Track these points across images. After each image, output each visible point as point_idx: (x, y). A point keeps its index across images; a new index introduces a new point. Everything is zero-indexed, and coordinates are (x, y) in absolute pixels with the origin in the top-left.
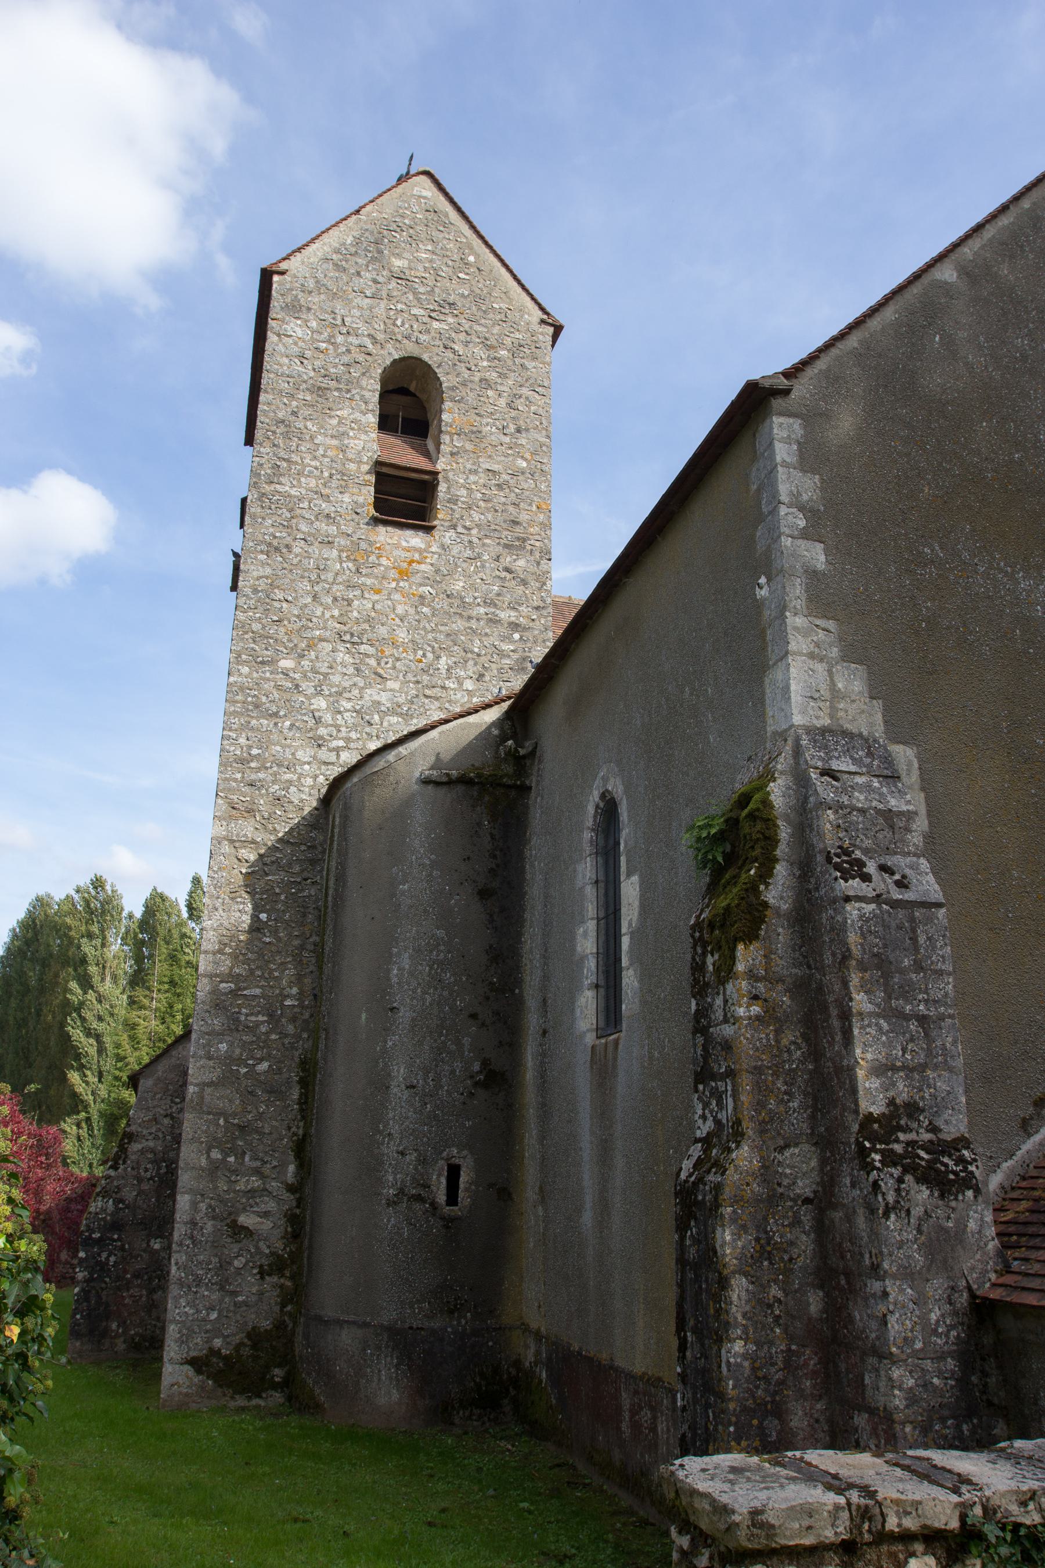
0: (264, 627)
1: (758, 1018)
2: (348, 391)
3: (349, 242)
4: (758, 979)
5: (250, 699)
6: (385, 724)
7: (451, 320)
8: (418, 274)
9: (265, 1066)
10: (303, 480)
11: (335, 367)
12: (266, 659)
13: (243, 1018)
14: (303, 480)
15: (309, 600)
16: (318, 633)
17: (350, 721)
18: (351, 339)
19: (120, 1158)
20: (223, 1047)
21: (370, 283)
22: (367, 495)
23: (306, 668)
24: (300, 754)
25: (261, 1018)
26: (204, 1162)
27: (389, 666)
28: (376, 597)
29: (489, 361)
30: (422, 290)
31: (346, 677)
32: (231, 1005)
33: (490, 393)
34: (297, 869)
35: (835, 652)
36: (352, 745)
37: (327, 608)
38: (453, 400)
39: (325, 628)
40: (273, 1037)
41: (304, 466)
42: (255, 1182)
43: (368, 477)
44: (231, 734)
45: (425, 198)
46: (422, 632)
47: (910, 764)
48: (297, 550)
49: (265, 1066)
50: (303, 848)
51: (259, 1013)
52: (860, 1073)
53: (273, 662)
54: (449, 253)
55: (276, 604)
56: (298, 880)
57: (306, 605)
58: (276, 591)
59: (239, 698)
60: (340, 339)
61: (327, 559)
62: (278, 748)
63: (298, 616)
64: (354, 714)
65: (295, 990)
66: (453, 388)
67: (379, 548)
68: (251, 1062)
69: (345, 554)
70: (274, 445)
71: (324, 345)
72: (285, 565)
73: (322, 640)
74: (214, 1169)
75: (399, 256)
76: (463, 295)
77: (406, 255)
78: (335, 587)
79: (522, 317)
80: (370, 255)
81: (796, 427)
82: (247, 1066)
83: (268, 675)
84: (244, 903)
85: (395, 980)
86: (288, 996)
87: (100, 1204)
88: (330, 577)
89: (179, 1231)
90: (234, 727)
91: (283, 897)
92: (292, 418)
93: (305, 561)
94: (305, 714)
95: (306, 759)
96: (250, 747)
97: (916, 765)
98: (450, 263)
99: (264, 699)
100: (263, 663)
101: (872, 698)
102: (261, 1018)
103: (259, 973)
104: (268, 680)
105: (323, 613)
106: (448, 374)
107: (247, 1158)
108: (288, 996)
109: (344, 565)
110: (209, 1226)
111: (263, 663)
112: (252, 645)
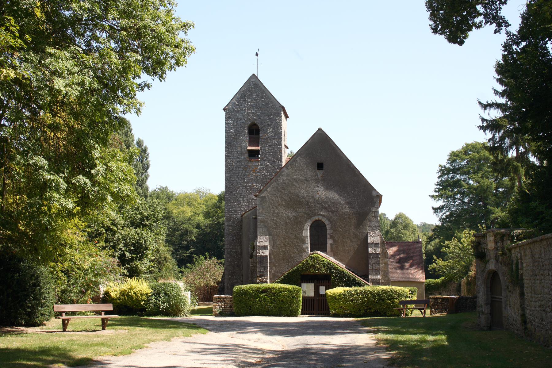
9: (236, 262)
18: (241, 121)
22: (247, 155)
24: (238, 209)
38: (262, 131)
42: (236, 281)
49: (236, 262)
53: (232, 192)
60: (239, 122)
74: (230, 279)
75: (249, 98)
77: (251, 98)
89: (225, 288)
110: (230, 287)
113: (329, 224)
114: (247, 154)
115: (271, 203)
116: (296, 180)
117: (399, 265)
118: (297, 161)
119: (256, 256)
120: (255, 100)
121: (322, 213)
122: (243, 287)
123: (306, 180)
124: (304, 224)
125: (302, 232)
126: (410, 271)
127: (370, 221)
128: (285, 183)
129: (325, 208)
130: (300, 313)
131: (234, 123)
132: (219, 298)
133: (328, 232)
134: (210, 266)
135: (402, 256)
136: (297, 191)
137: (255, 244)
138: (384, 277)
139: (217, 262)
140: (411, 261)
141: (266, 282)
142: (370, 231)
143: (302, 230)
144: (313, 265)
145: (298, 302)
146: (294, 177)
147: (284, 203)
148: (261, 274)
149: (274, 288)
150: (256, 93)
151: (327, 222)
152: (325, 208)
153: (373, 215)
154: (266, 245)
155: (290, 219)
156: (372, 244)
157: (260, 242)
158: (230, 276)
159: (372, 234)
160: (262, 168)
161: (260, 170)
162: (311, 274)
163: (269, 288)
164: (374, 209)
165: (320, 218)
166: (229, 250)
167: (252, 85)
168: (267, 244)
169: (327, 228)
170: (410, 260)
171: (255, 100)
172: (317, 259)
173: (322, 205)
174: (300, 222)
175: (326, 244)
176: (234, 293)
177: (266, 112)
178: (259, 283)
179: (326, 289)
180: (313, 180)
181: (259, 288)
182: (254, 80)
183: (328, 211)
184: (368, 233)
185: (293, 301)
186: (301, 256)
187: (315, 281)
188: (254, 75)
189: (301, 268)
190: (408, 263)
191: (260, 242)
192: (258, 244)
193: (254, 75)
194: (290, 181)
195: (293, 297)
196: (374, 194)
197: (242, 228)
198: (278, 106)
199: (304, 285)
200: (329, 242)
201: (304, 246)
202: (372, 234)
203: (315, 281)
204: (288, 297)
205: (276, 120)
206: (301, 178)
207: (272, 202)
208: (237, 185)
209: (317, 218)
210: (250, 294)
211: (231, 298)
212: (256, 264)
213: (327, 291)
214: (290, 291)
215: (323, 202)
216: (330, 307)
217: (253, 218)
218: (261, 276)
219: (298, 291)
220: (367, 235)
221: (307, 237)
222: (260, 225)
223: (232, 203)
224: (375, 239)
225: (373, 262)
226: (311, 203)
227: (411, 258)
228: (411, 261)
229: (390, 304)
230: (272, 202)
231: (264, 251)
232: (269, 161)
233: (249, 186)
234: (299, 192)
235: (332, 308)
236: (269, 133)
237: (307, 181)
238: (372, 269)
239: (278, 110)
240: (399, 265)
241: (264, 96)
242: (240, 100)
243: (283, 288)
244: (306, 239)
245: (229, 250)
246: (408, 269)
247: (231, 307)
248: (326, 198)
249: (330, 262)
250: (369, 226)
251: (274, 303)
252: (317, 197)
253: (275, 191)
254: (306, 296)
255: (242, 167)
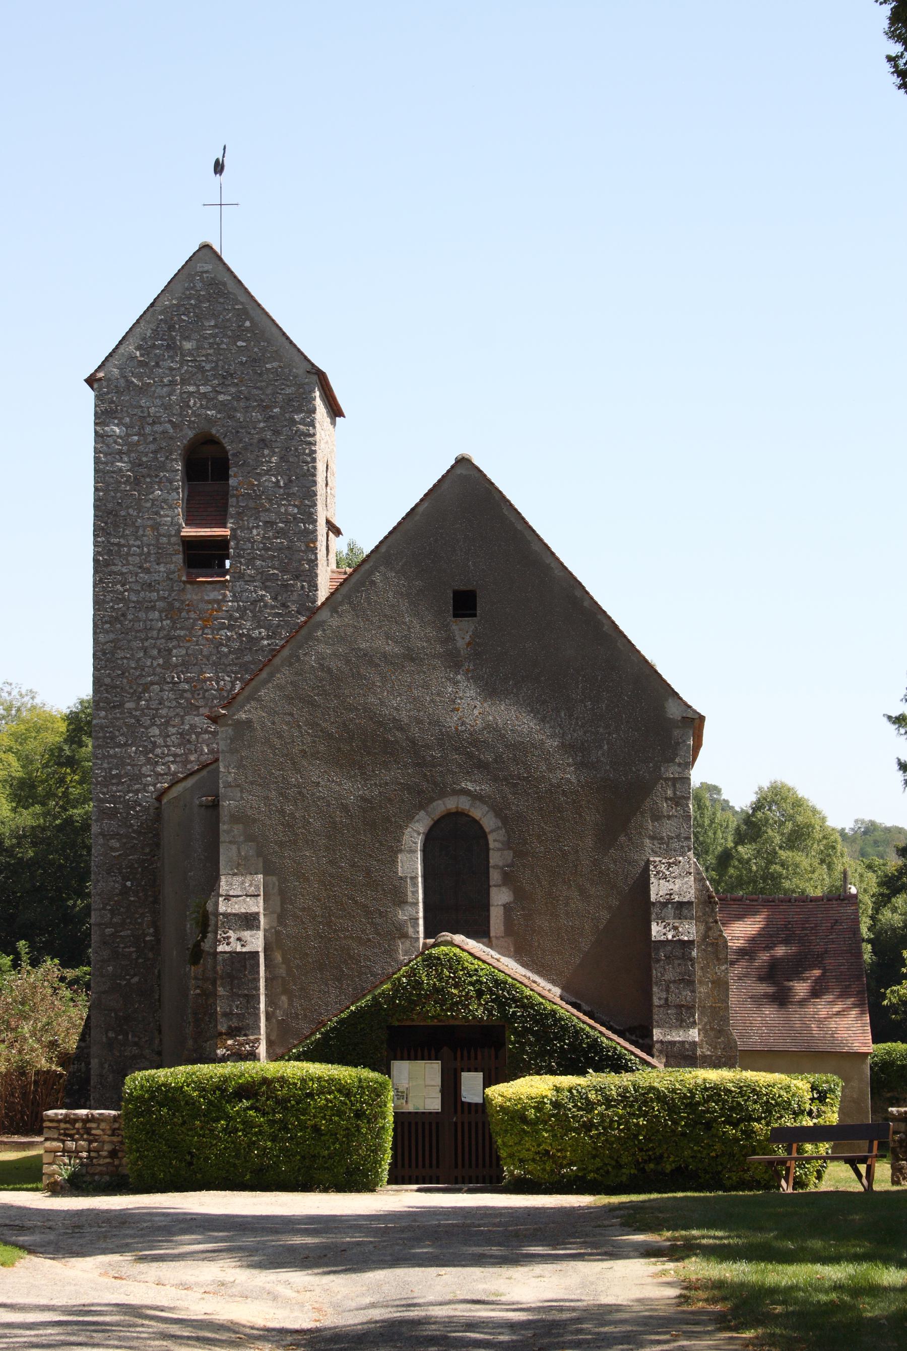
0: (112, 680)
1: (198, 994)
2: (157, 476)
3: (148, 335)
4: (198, 979)
5: (108, 735)
6: (200, 740)
7: (233, 390)
8: (204, 352)
10: (130, 558)
11: (146, 455)
12: (116, 704)
13: (120, 950)
14: (130, 558)
15: (142, 655)
16: (149, 679)
17: (176, 741)
19: (86, 1034)
20: (110, 968)
21: (167, 372)
22: (179, 558)
23: (143, 707)
25: (132, 949)
26: (104, 1040)
27: (200, 696)
28: (188, 644)
29: (265, 422)
30: (208, 367)
31: (172, 709)
32: (113, 942)
33: (266, 452)
34: (147, 850)
35: (242, 838)
36: (178, 759)
37: (154, 658)
39: (154, 674)
40: (140, 961)
41: (129, 547)
42: (136, 1051)
43: (176, 547)
44: (98, 761)
45: (206, 272)
46: (223, 667)
47: (274, 884)
48: (130, 617)
50: (151, 835)
51: (130, 946)
52: (219, 1017)
53: (121, 705)
54: (228, 324)
55: (119, 662)
56: (149, 857)
57: (139, 659)
58: (118, 651)
59: (101, 735)
61: (152, 620)
62: (129, 767)
63: (135, 669)
64: (178, 736)
65: (152, 930)
66: (234, 455)
67: (188, 605)
68: (128, 977)
69: (163, 615)
70: (108, 534)
71: (136, 438)
72: (123, 630)
73: (152, 683)
75: (187, 338)
76: (241, 363)
77: (196, 336)
78: (159, 642)
79: (290, 371)
80: (165, 343)
81: (230, 731)
82: (125, 980)
83: (118, 715)
84: (115, 876)
85: (189, 931)
86: (148, 934)
87: (76, 1066)
88: (155, 633)
89: (94, 1080)
90: (100, 756)
91: (140, 869)
92: (118, 508)
93: (136, 625)
94: (145, 741)
95: (148, 773)
96: (111, 769)
97: (277, 884)
98: (229, 333)
99: (117, 733)
100: (114, 707)
101: (258, 857)
102: (132, 949)
103: (128, 921)
104: (119, 718)
105: (152, 662)
106: (232, 442)
107: (130, 1036)
108: (148, 934)
109: (164, 623)
110: (110, 1078)
111: (114, 707)
112: (106, 695)
113: (498, 828)
114: (181, 556)
115: (272, 747)
116: (367, 658)
117: (771, 990)
118: (373, 583)
119: (215, 954)
120: (211, 345)
121: (470, 787)
122: (162, 1075)
123: (411, 657)
124: (401, 828)
125: (394, 862)
126: (811, 1010)
127: (657, 817)
128: (329, 671)
129: (483, 766)
130: (385, 1176)
131: (128, 435)
132: (66, 1119)
133: (495, 858)
134: (34, 994)
135: (780, 951)
136: (371, 699)
137: (210, 907)
138: (712, 1034)
139: (62, 979)
140: (817, 972)
141: (252, 1056)
142: (655, 853)
143: (395, 851)
144: (436, 990)
145: (378, 1136)
146: (363, 646)
147: (322, 748)
148: (234, 1023)
149: (283, 1080)
150: (215, 316)
151: (489, 822)
152: (483, 766)
153: (670, 793)
154: (254, 909)
155: (345, 808)
156: (664, 905)
157: (228, 898)
158: (111, 1034)
159: (663, 868)
160: (238, 609)
161: (231, 618)
162: (429, 1022)
163: (265, 1081)
164: (671, 771)
165: (464, 803)
166: (108, 931)
167: (199, 285)
168: (257, 906)
169: (492, 845)
170: (812, 967)
171: (211, 345)
172: (454, 963)
173: (470, 756)
174: (388, 819)
175: (486, 907)
176: (128, 1101)
177: (255, 392)
178: (223, 1059)
179: (488, 1083)
180: (434, 657)
181: (226, 1079)
182: (208, 267)
183: (496, 779)
184: (648, 862)
185: (358, 1129)
186: (391, 952)
187: (445, 1050)
188: (206, 248)
189: (390, 1000)
190: (804, 980)
191: (228, 898)
192: (222, 908)
193: (206, 248)
194: (348, 662)
195: (359, 1114)
196: (673, 711)
197: (158, 845)
198: (300, 371)
199: (402, 1069)
200: (500, 897)
201: (402, 916)
202: (663, 868)
203: (445, 1050)
204: (340, 1113)
205: (293, 422)
206: (391, 648)
207: (276, 742)
208: (141, 676)
209: (451, 804)
210: (191, 1102)
211: (115, 1119)
212: (214, 983)
213: (489, 1091)
214: (344, 1090)
215: (475, 743)
216: (503, 1154)
217: (201, 806)
218: (232, 1033)
219: (377, 1092)
220: (646, 870)
221: (413, 879)
222: (228, 832)
223: (120, 746)
224: (676, 888)
225: (670, 975)
226: (427, 747)
227: (817, 960)
228: (817, 972)
229: (736, 1140)
230: (276, 742)
231: (246, 934)
232: (266, 581)
233: (187, 681)
234: (382, 703)
235: (511, 1156)
236: (267, 472)
237: (412, 660)
238: (667, 1004)
239: (301, 386)
240: (771, 990)
241: (247, 330)
242: (154, 346)
243: (319, 1079)
244: (410, 889)
245: (108, 931)
246: (803, 1003)
247: (113, 1154)
248: (488, 727)
249: (501, 976)
250: (652, 838)
251: (283, 1140)
252: (451, 721)
253: (289, 699)
254: (410, 1108)
255: (160, 604)
